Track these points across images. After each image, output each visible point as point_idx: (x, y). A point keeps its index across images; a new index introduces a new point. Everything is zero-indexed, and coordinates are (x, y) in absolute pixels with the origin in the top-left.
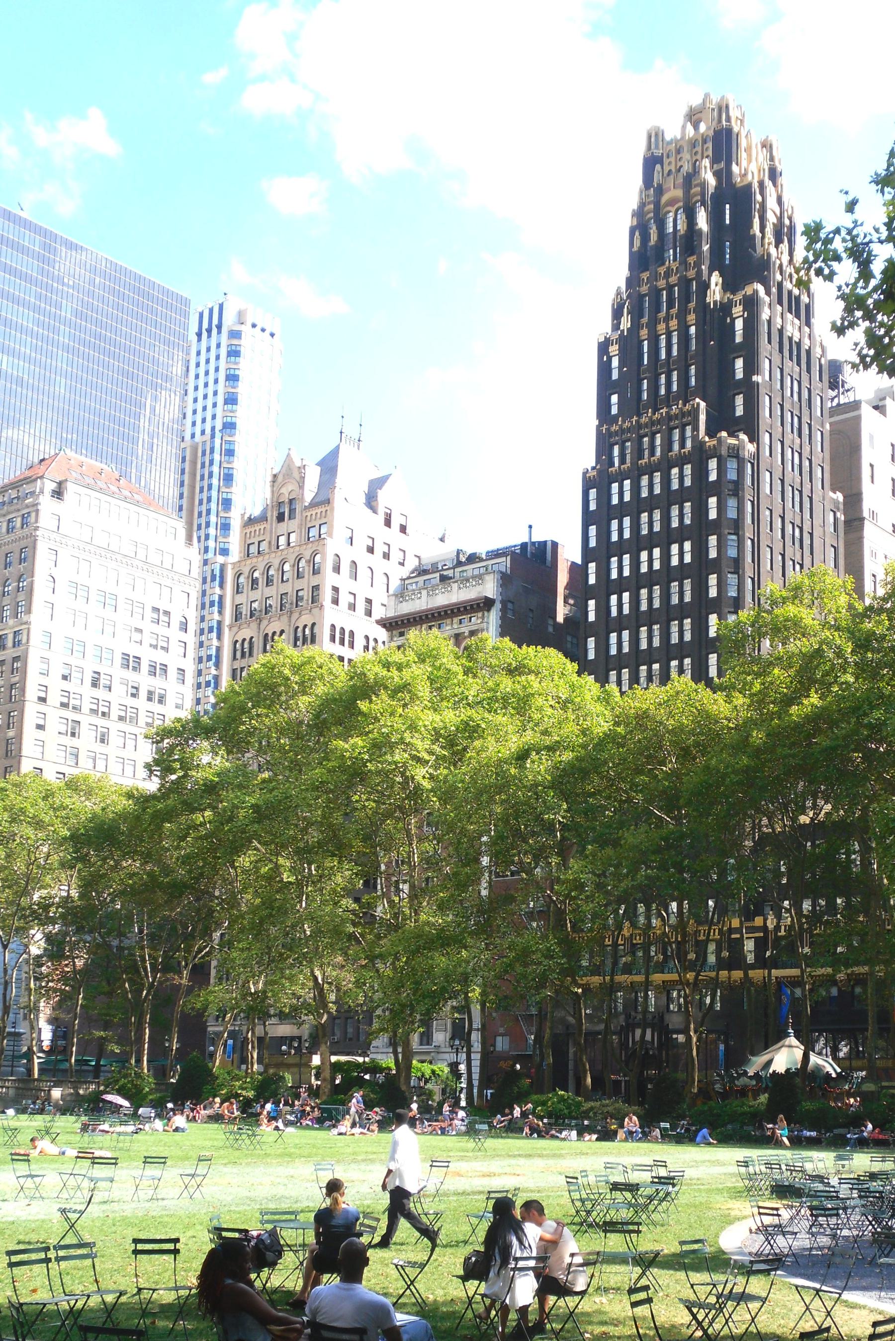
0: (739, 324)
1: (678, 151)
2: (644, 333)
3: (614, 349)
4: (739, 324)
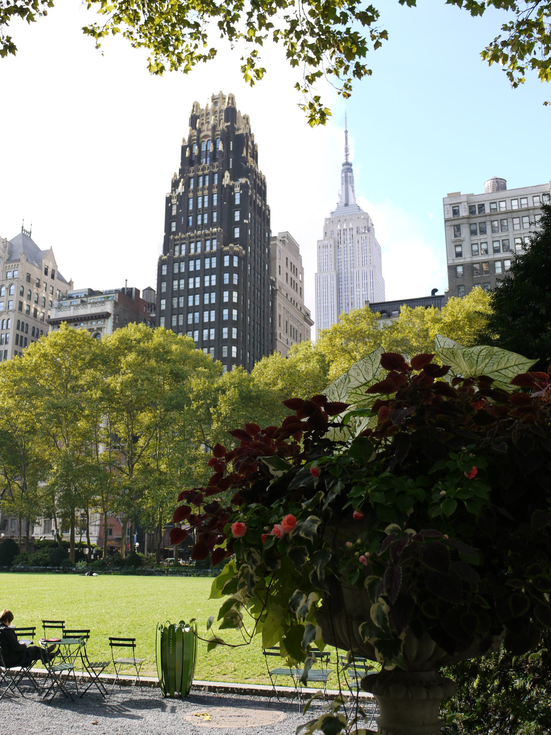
0: (237, 196)
1: (208, 114)
2: (191, 195)
3: (174, 201)
4: (237, 196)
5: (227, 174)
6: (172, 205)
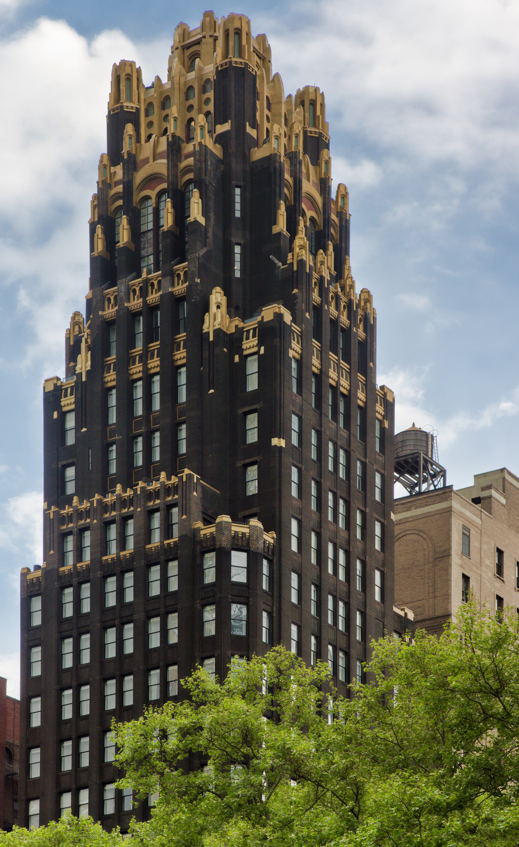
0: (252, 367)
2: (111, 377)
3: (68, 402)
4: (252, 367)
5: (217, 296)
6: (63, 415)
